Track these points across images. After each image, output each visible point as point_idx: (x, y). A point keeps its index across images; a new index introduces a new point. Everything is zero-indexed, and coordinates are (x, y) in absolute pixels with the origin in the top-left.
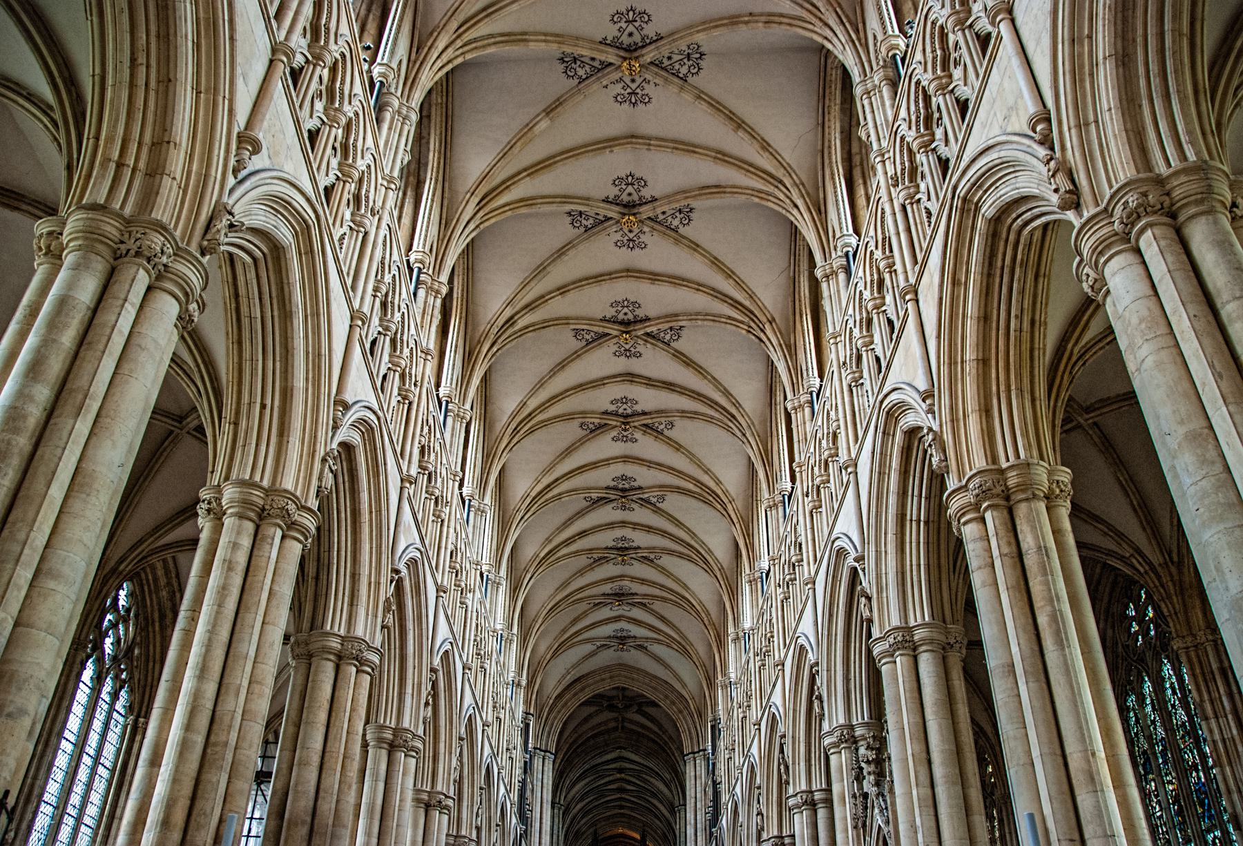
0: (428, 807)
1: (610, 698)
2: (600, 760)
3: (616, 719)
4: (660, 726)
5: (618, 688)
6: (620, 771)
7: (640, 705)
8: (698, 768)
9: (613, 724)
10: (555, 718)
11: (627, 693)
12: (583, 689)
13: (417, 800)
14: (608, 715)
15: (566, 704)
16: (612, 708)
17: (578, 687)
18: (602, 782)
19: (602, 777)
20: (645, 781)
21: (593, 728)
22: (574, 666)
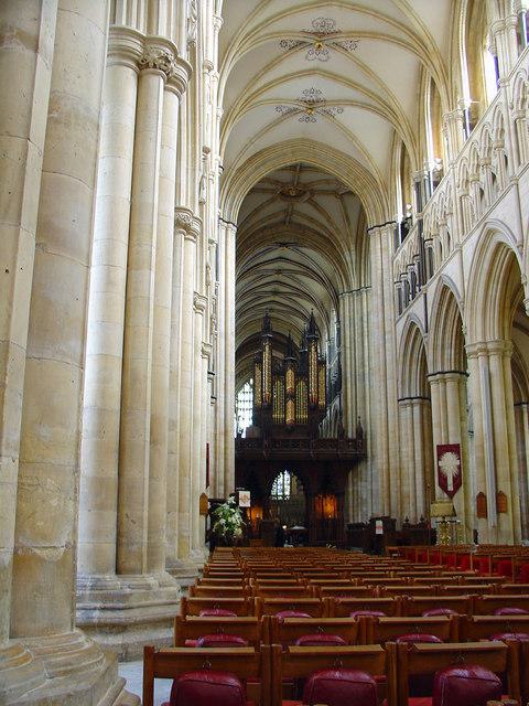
0: (142, 67)
1: (283, 185)
2: (262, 260)
3: (286, 211)
4: (329, 219)
5: (293, 168)
6: (279, 272)
7: (313, 192)
8: (384, 241)
9: (282, 217)
10: (237, 190)
11: (306, 177)
12: (264, 163)
13: (119, 53)
14: (280, 205)
15: (248, 177)
16: (285, 195)
17: (260, 160)
18: (261, 283)
19: (262, 277)
20: (299, 282)
21: (262, 221)
22: (258, 136)
